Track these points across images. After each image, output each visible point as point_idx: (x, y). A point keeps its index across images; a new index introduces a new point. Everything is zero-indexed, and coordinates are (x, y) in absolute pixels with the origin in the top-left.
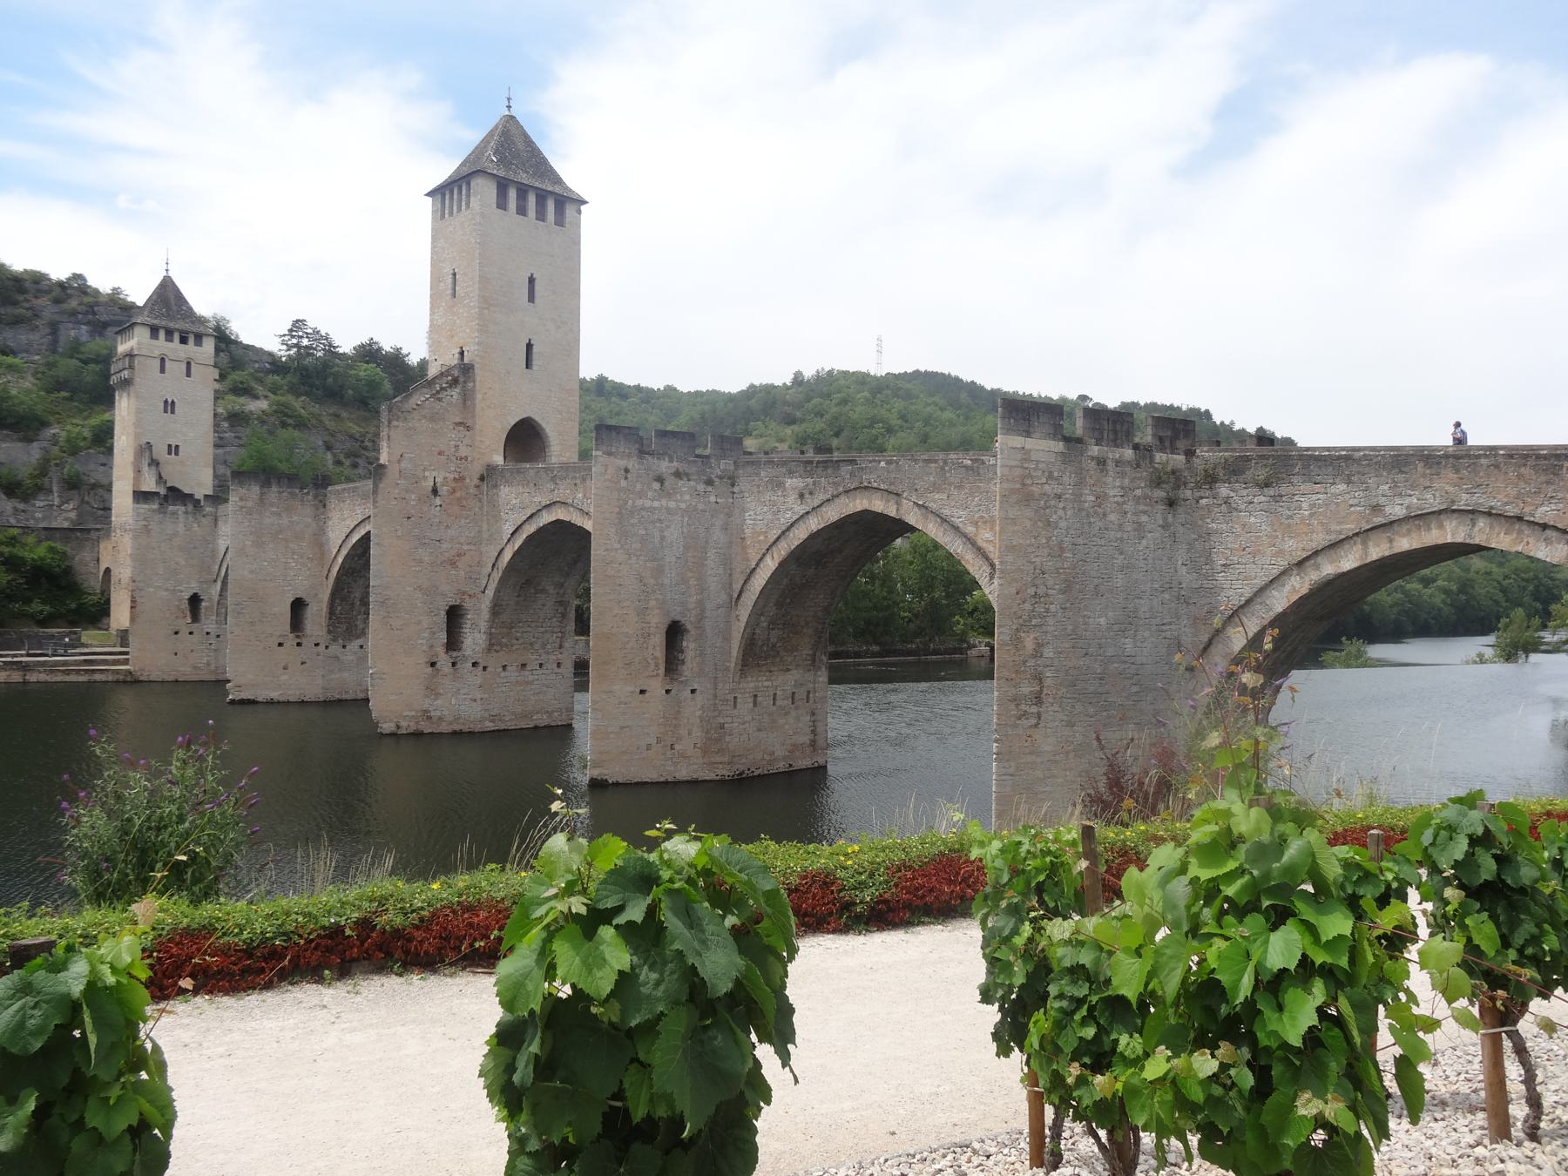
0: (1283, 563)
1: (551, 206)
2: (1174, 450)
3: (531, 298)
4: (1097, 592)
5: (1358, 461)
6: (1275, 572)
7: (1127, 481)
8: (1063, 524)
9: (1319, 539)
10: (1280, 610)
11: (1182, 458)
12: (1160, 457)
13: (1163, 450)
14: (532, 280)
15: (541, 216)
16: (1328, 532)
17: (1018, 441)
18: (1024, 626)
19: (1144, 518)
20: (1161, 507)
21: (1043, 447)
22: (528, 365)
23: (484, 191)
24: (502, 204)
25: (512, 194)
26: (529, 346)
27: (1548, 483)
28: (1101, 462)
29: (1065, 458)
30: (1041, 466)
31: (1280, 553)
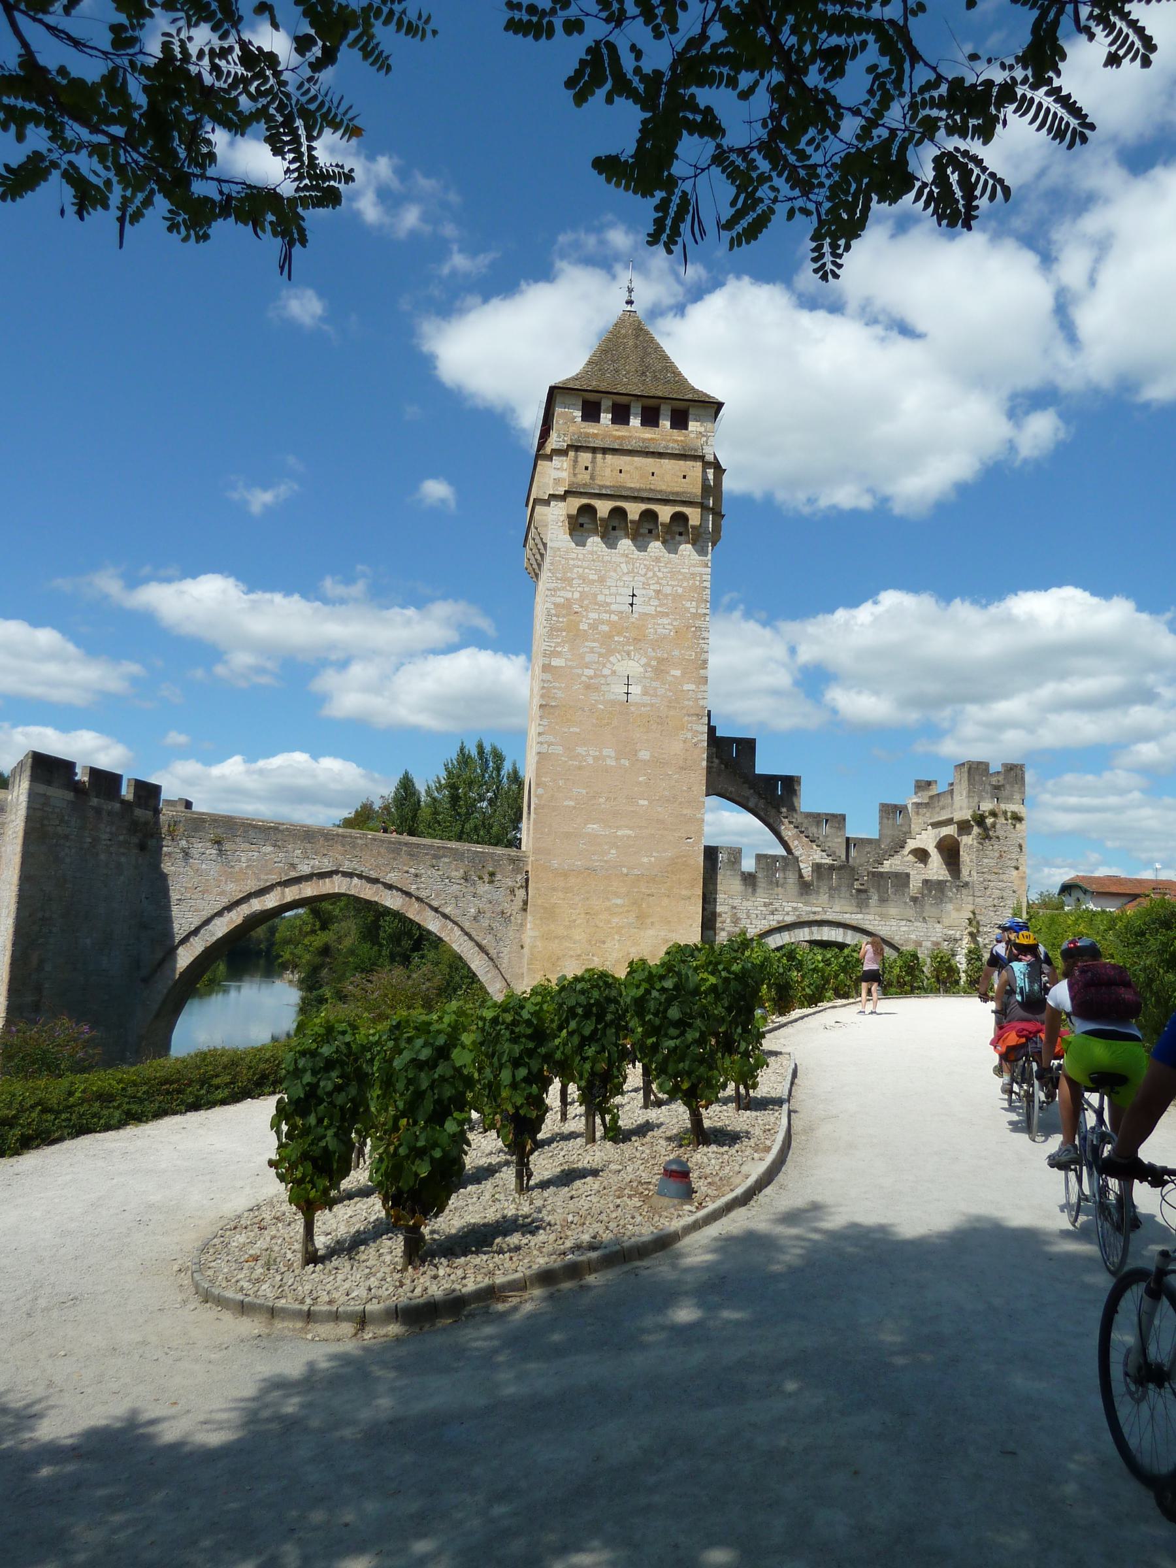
0: (224, 901)
5: (282, 831)
6: (219, 907)
7: (114, 829)
8: (68, 860)
9: (252, 885)
10: (220, 935)
11: (151, 813)
12: (138, 812)
13: (139, 806)
16: (259, 880)
19: (123, 859)
20: (135, 851)
27: (394, 859)
30: (57, 810)
31: (222, 893)
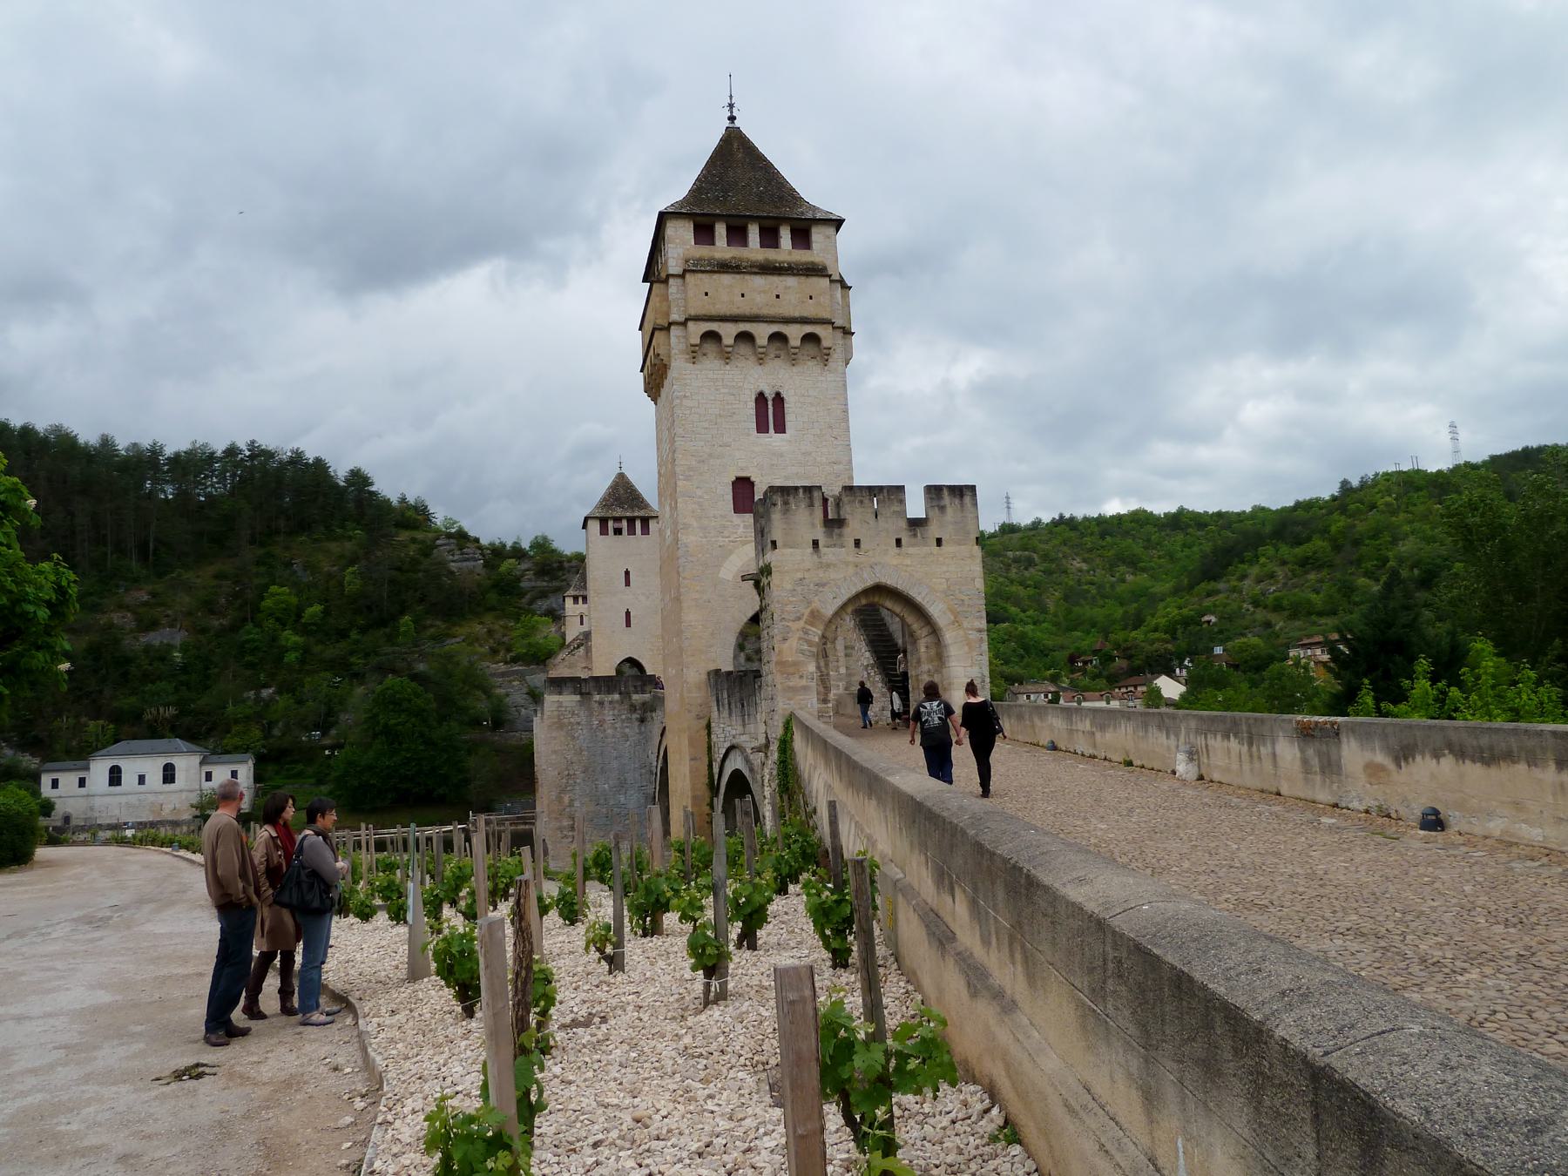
1: (638, 524)
2: (643, 692)
3: (628, 583)
4: (603, 771)
12: (635, 697)
14: (627, 573)
15: (632, 531)
17: (555, 698)
18: (563, 791)
21: (569, 699)
22: (628, 624)
23: (595, 526)
24: (604, 531)
25: (610, 523)
26: (628, 614)
28: (601, 703)
29: (581, 703)
